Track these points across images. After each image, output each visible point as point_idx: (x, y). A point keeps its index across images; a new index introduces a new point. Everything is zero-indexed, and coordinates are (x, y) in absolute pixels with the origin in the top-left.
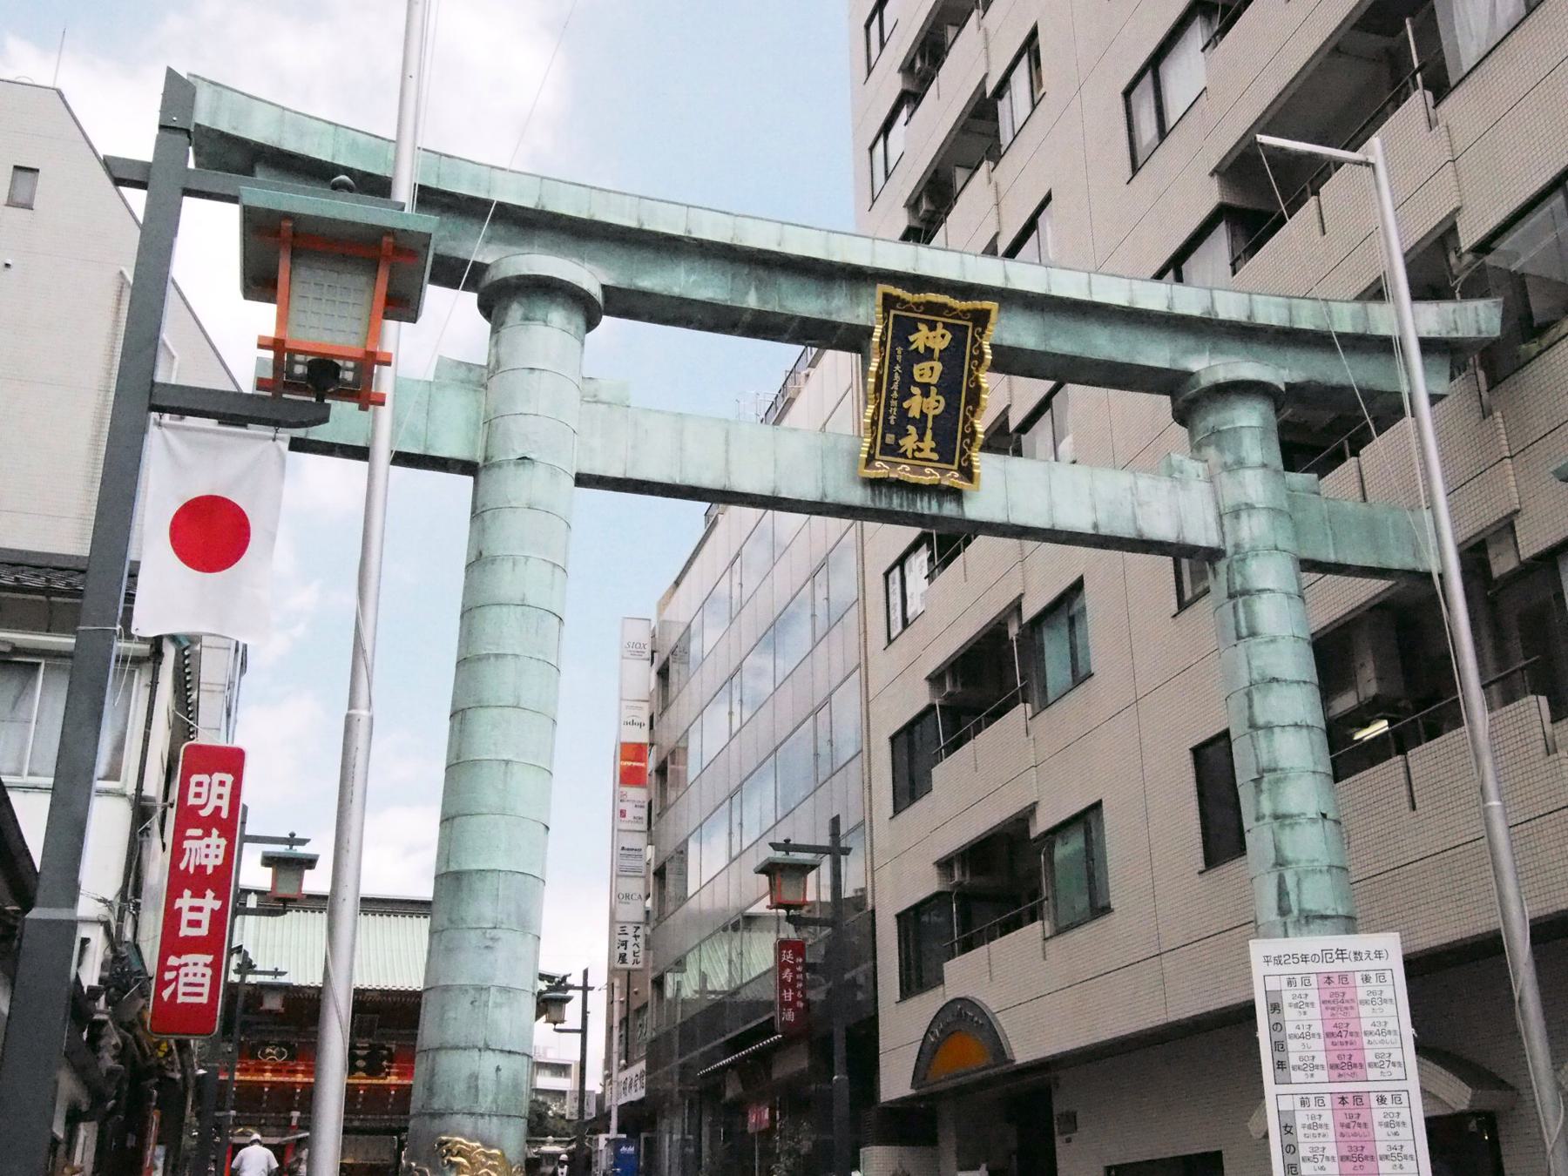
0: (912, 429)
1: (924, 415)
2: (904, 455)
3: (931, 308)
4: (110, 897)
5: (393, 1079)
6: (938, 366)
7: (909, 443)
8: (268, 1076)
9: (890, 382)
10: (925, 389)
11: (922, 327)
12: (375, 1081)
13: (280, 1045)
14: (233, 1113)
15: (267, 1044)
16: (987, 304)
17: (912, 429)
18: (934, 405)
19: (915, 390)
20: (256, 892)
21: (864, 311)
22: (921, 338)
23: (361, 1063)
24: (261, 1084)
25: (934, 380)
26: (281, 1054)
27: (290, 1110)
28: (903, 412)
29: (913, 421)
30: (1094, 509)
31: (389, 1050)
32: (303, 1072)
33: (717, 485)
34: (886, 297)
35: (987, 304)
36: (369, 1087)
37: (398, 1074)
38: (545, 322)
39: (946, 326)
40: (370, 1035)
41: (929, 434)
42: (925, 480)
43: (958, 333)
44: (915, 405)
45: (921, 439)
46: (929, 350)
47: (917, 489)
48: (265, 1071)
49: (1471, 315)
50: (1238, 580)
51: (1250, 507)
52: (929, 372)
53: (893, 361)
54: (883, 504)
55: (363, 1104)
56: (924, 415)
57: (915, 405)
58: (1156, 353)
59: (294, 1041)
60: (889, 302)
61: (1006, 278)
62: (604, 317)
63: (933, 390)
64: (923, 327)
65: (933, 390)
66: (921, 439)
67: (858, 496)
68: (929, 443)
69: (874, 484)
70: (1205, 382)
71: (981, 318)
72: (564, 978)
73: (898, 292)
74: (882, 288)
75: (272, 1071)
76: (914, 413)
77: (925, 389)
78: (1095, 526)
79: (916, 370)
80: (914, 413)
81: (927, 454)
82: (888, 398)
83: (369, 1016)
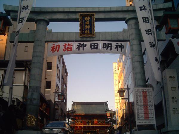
0: (86, 30)
1: (87, 28)
2: (85, 33)
3: (86, 15)
4: (22, 96)
5: (94, 125)
6: (89, 22)
7: (86, 32)
9: (83, 24)
10: (87, 25)
11: (86, 17)
16: (93, 13)
17: (86, 30)
18: (89, 27)
19: (86, 25)
21: (78, 16)
22: (86, 19)
25: (88, 24)
28: (85, 28)
29: (86, 29)
30: (111, 37)
33: (62, 40)
34: (81, 15)
35: (93, 13)
38: (41, 24)
39: (89, 17)
41: (88, 30)
42: (88, 36)
43: (91, 18)
44: (86, 27)
45: (87, 31)
46: (87, 20)
47: (87, 37)
49: (167, 5)
50: (131, 44)
51: (133, 34)
52: (87, 23)
53: (83, 22)
54: (83, 40)
56: (87, 28)
57: (86, 27)
58: (120, 16)
60: (81, 15)
61: (99, 9)
62: (50, 23)
63: (88, 25)
64: (86, 17)
65: (88, 25)
66: (87, 31)
67: (80, 39)
68: (88, 31)
69: (81, 37)
70: (127, 19)
71: (93, 15)
73: (82, 14)
74: (80, 13)
76: (86, 28)
77: (87, 25)
78: (112, 39)
79: (86, 23)
80: (86, 28)
81: (88, 33)
82: (83, 27)
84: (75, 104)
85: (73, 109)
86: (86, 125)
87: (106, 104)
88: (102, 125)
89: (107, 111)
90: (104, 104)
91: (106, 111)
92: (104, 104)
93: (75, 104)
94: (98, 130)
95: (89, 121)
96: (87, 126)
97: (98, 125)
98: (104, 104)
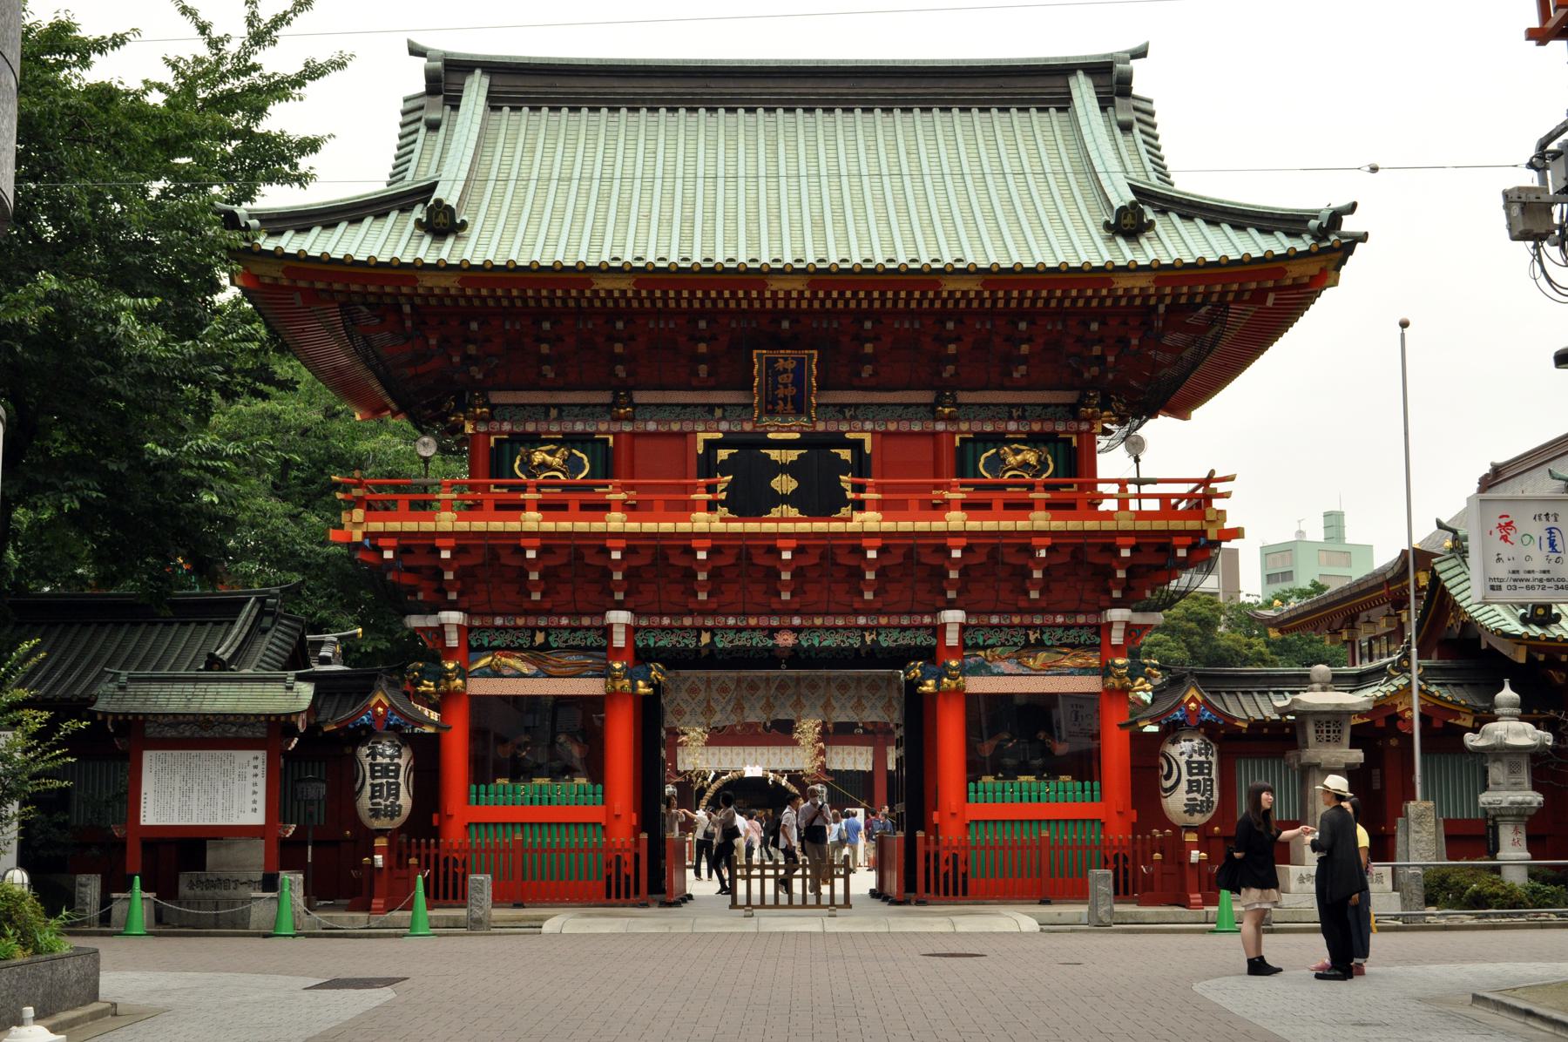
5: (870, 521)
8: (532, 520)
12: (820, 526)
13: (569, 440)
14: (453, 617)
15: (535, 440)
20: (493, 68)
23: (784, 484)
24: (515, 542)
26: (573, 465)
27: (603, 615)
31: (857, 446)
32: (628, 508)
36: (803, 543)
37: (881, 506)
40: (800, 407)
48: (521, 507)
55: (797, 589)
59: (603, 428)
72: (1336, 217)
75: (541, 507)
83: (786, 359)
84: (475, 91)
85: (410, 182)
86: (702, 522)
87: (1105, 104)
88: (1040, 520)
89: (1150, 214)
90: (1083, 91)
91: (1127, 225)
92: (1064, 103)
93: (475, 91)
94: (953, 617)
95: (750, 445)
96: (718, 543)
97: (956, 520)
98: (1083, 91)
